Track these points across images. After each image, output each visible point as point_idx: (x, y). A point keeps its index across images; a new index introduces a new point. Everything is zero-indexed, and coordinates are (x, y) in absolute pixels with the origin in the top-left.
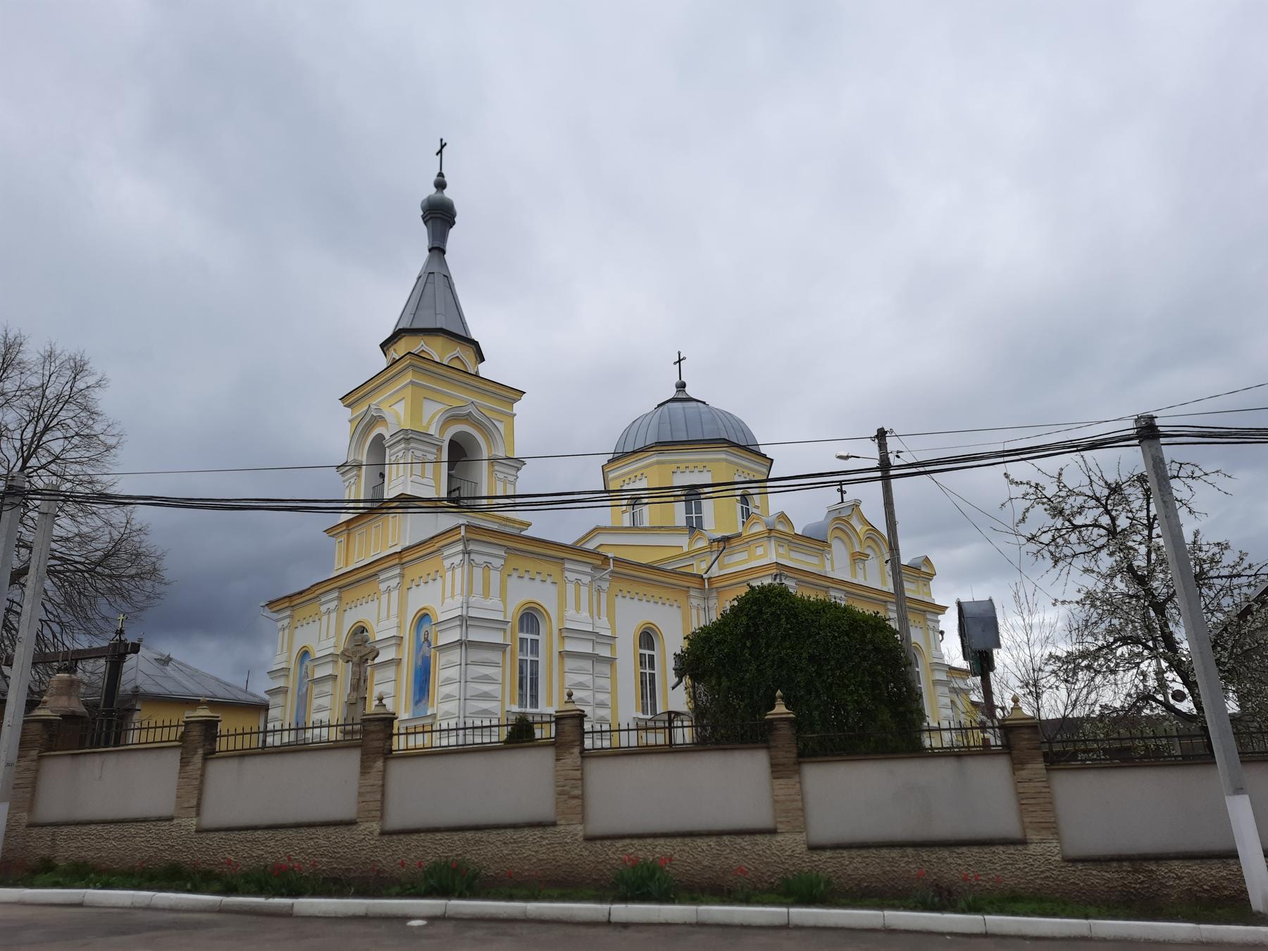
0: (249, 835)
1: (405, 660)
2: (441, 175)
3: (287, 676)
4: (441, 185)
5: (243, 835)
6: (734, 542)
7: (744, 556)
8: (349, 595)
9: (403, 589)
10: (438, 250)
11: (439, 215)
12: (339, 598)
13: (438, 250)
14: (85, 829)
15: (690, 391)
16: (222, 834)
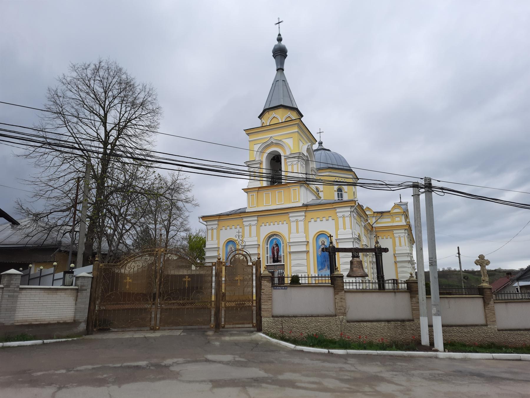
0: (519, 332)
1: (310, 251)
2: (279, 35)
3: (218, 251)
4: (280, 40)
5: (516, 332)
6: (384, 214)
7: (389, 220)
8: (262, 219)
9: (307, 222)
10: (280, 69)
11: (280, 53)
12: (258, 220)
13: (280, 69)
14: (451, 328)
15: (325, 146)
16: (508, 332)
